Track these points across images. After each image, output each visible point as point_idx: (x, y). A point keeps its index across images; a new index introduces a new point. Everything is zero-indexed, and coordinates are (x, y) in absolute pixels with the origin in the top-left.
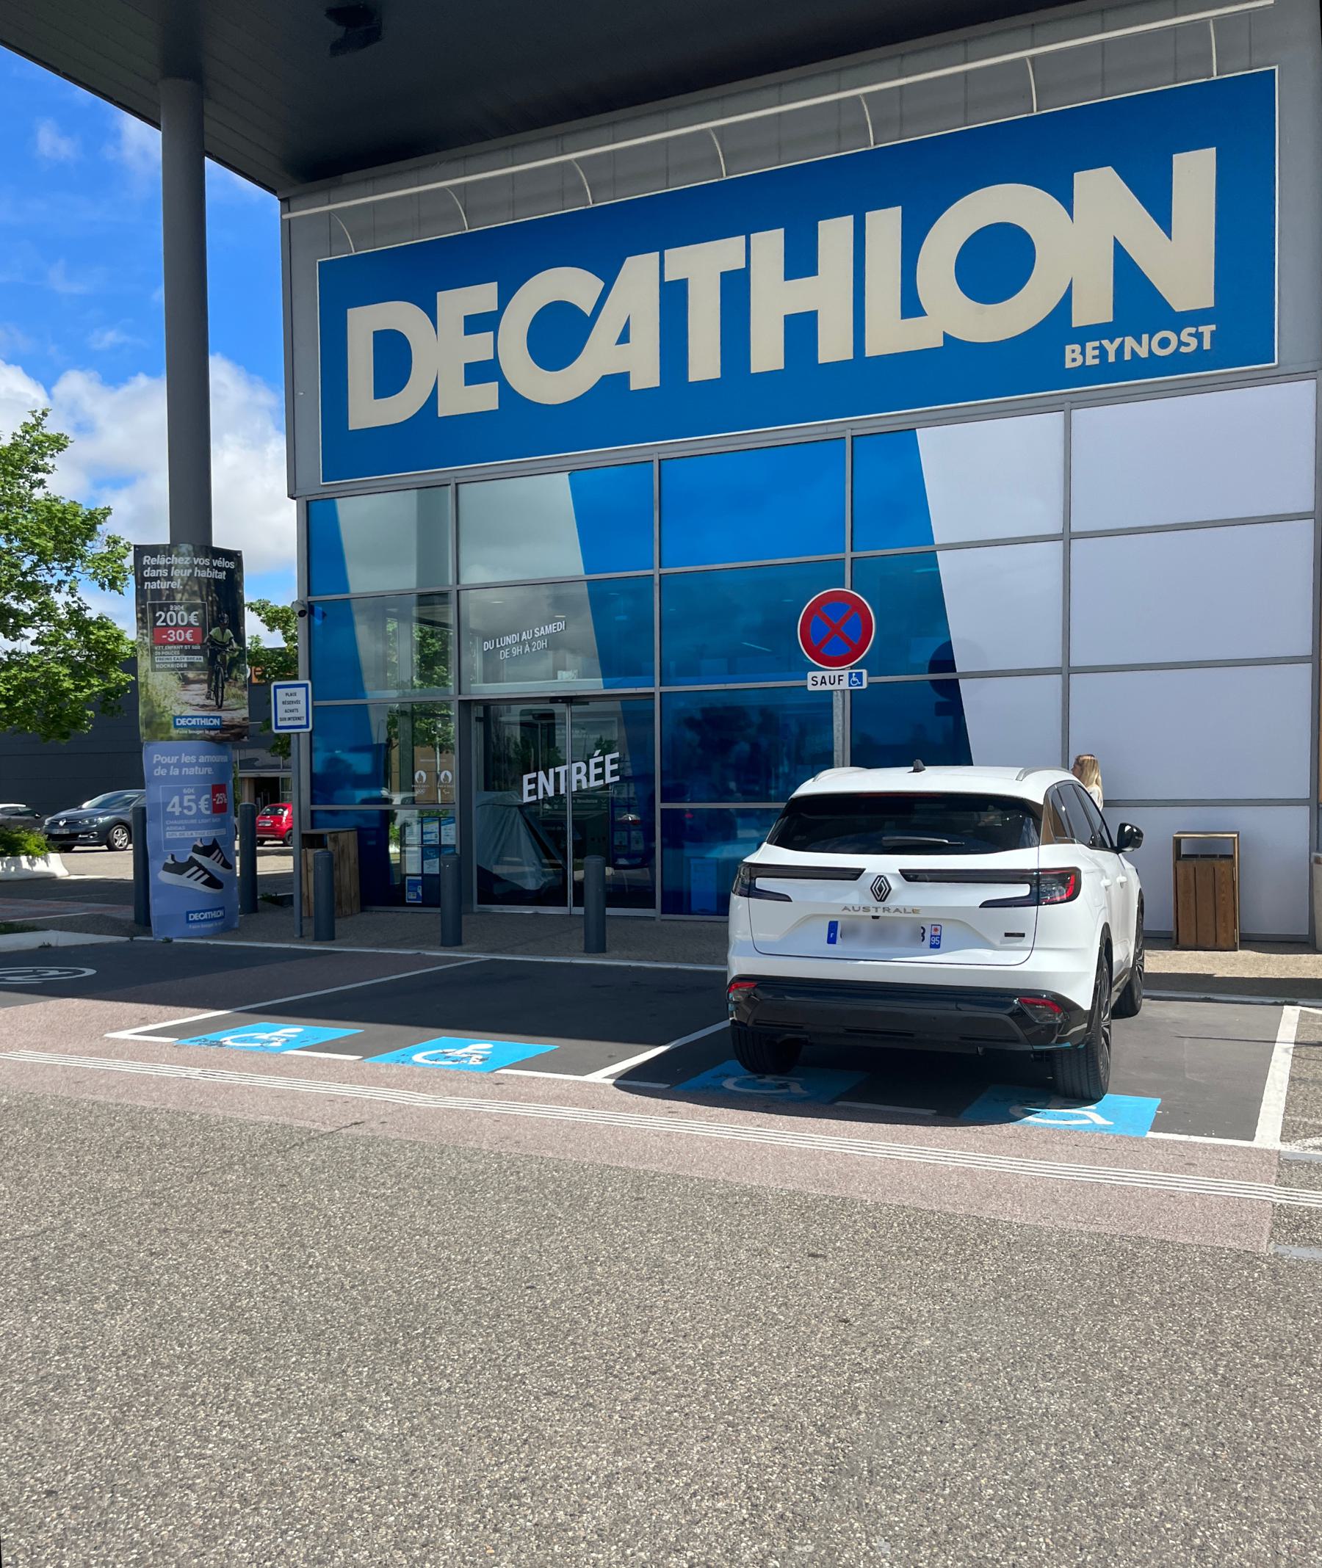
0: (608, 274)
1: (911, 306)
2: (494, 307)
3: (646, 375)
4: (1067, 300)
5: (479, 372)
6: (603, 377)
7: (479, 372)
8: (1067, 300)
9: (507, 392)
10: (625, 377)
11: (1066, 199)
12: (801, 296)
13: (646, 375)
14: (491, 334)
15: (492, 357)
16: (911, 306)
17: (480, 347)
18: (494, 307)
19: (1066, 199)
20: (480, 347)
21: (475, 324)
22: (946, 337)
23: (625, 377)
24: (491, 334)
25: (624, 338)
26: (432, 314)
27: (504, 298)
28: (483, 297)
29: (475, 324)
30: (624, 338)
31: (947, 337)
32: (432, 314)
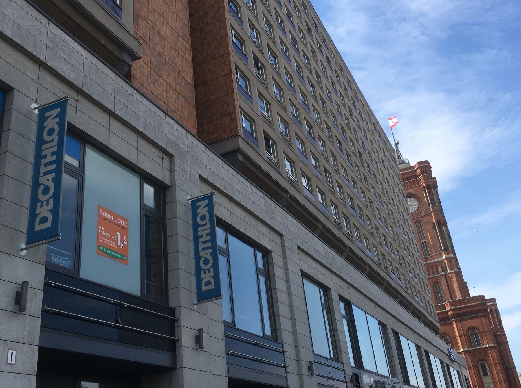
0: (201, 257)
1: (206, 225)
3: (210, 251)
4: (206, 211)
5: (209, 272)
6: (210, 255)
7: (209, 272)
8: (206, 211)
9: (211, 267)
10: (210, 253)
11: (199, 213)
12: (204, 236)
13: (210, 251)
15: (208, 270)
16: (206, 225)
17: (207, 271)
19: (199, 213)
20: (207, 271)
21: (205, 273)
22: (209, 220)
23: (210, 253)
26: (203, 278)
27: (203, 269)
28: (202, 272)
29: (205, 273)
30: (207, 254)
32: (203, 278)
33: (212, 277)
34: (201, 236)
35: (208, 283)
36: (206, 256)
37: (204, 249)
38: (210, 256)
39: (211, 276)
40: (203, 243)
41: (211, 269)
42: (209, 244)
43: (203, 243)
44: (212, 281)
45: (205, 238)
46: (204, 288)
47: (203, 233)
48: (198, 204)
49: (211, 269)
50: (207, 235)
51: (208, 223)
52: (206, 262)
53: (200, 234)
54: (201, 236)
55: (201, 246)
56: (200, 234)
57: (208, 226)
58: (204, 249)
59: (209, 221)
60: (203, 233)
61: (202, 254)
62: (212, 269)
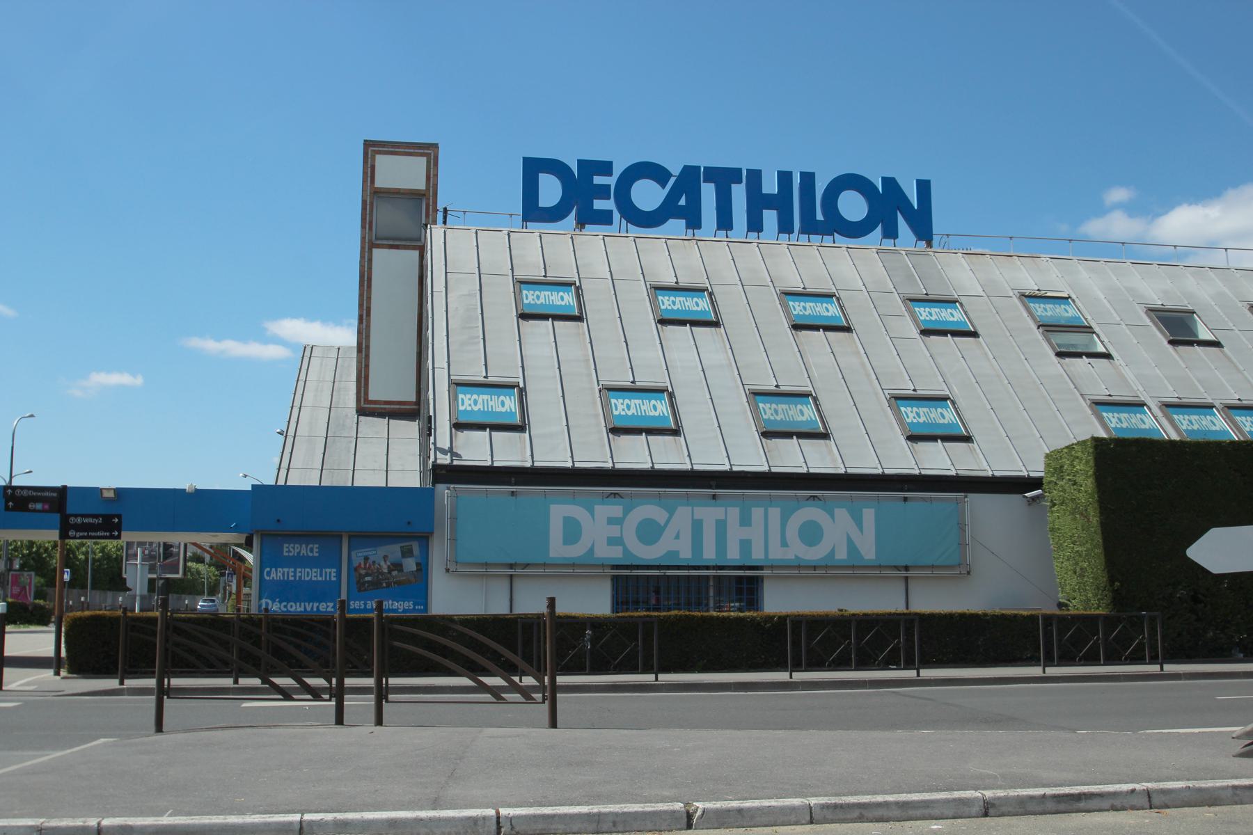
1: (784, 543)
2: (621, 515)
4: (833, 551)
5: (612, 541)
6: (669, 551)
7: (612, 541)
9: (626, 551)
10: (678, 552)
14: (619, 526)
15: (619, 535)
16: (784, 543)
18: (621, 516)
19: (832, 516)
20: (615, 531)
21: (611, 521)
22: (796, 556)
23: (678, 552)
24: (619, 526)
25: (677, 537)
26: (593, 516)
27: (627, 511)
29: (611, 521)
30: (677, 537)
31: (796, 556)
32: (593, 516)
33: (591, 551)
34: (745, 521)
35: (572, 531)
36: (668, 535)
37: (697, 526)
38: (665, 552)
39: (593, 545)
40: (721, 526)
41: (621, 548)
43: (721, 526)
44: (575, 552)
45: (735, 534)
47: (754, 533)
48: (869, 515)
49: (621, 548)
52: (649, 532)
53: (757, 513)
54: (745, 521)
56: (757, 513)
58: (697, 526)
59: (793, 557)
60: (754, 533)
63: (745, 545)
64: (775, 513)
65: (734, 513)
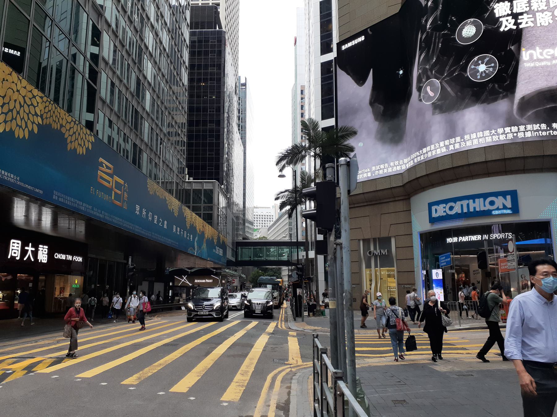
0: (455, 203)
1: (485, 206)
3: (460, 212)
9: (447, 213)
12: (475, 205)
16: (485, 206)
27: (446, 205)
29: (444, 208)
34: (474, 202)
37: (462, 206)
40: (468, 205)
42: (465, 210)
43: (468, 205)
46: (433, 208)
50: (475, 208)
51: (486, 209)
52: (451, 208)
53: (477, 200)
54: (474, 202)
55: (465, 203)
57: (483, 208)
58: (462, 206)
61: (459, 203)
62: (445, 214)
63: (475, 208)
64: (482, 200)
65: (471, 201)
